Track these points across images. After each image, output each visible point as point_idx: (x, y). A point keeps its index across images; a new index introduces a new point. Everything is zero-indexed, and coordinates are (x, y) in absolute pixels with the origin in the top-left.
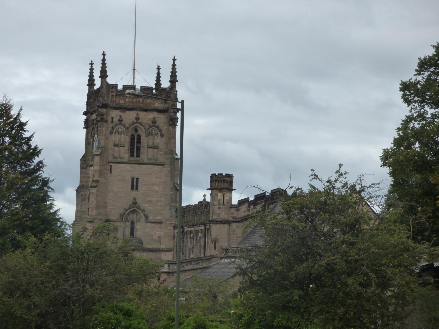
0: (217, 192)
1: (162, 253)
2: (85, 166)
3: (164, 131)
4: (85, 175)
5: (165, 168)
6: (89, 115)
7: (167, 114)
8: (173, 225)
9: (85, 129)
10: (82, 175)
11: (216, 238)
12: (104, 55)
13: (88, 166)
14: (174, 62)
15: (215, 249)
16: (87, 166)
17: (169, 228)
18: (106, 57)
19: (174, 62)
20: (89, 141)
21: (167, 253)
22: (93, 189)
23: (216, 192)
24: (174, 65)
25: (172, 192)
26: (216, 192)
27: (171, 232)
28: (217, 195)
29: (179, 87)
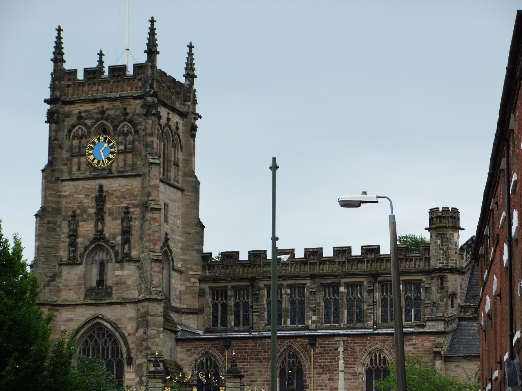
0: (452, 231)
1: (183, 315)
2: (53, 179)
3: (183, 142)
4: (54, 192)
5: (185, 195)
6: (60, 104)
7: (185, 119)
8: (198, 276)
9: (48, 124)
10: (48, 192)
11: (453, 292)
12: (152, 21)
13: (58, 180)
14: (191, 51)
15: (452, 306)
16: (57, 179)
17: (192, 280)
18: (156, 25)
19: (191, 51)
20: (60, 142)
21: (190, 316)
22: (155, 212)
23: (451, 232)
24: (190, 54)
25: (196, 231)
26: (451, 232)
27: (196, 286)
28: (453, 236)
29: (197, 84)
